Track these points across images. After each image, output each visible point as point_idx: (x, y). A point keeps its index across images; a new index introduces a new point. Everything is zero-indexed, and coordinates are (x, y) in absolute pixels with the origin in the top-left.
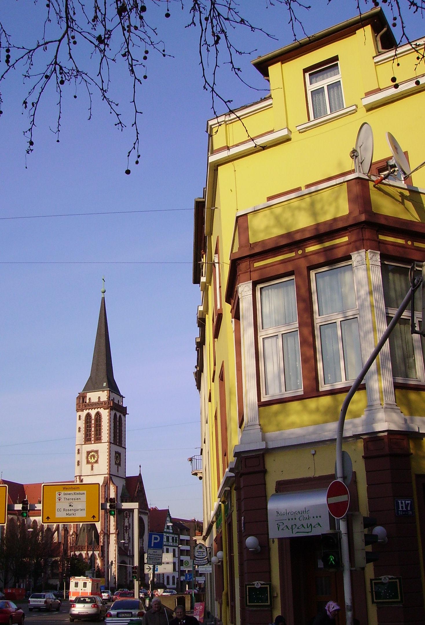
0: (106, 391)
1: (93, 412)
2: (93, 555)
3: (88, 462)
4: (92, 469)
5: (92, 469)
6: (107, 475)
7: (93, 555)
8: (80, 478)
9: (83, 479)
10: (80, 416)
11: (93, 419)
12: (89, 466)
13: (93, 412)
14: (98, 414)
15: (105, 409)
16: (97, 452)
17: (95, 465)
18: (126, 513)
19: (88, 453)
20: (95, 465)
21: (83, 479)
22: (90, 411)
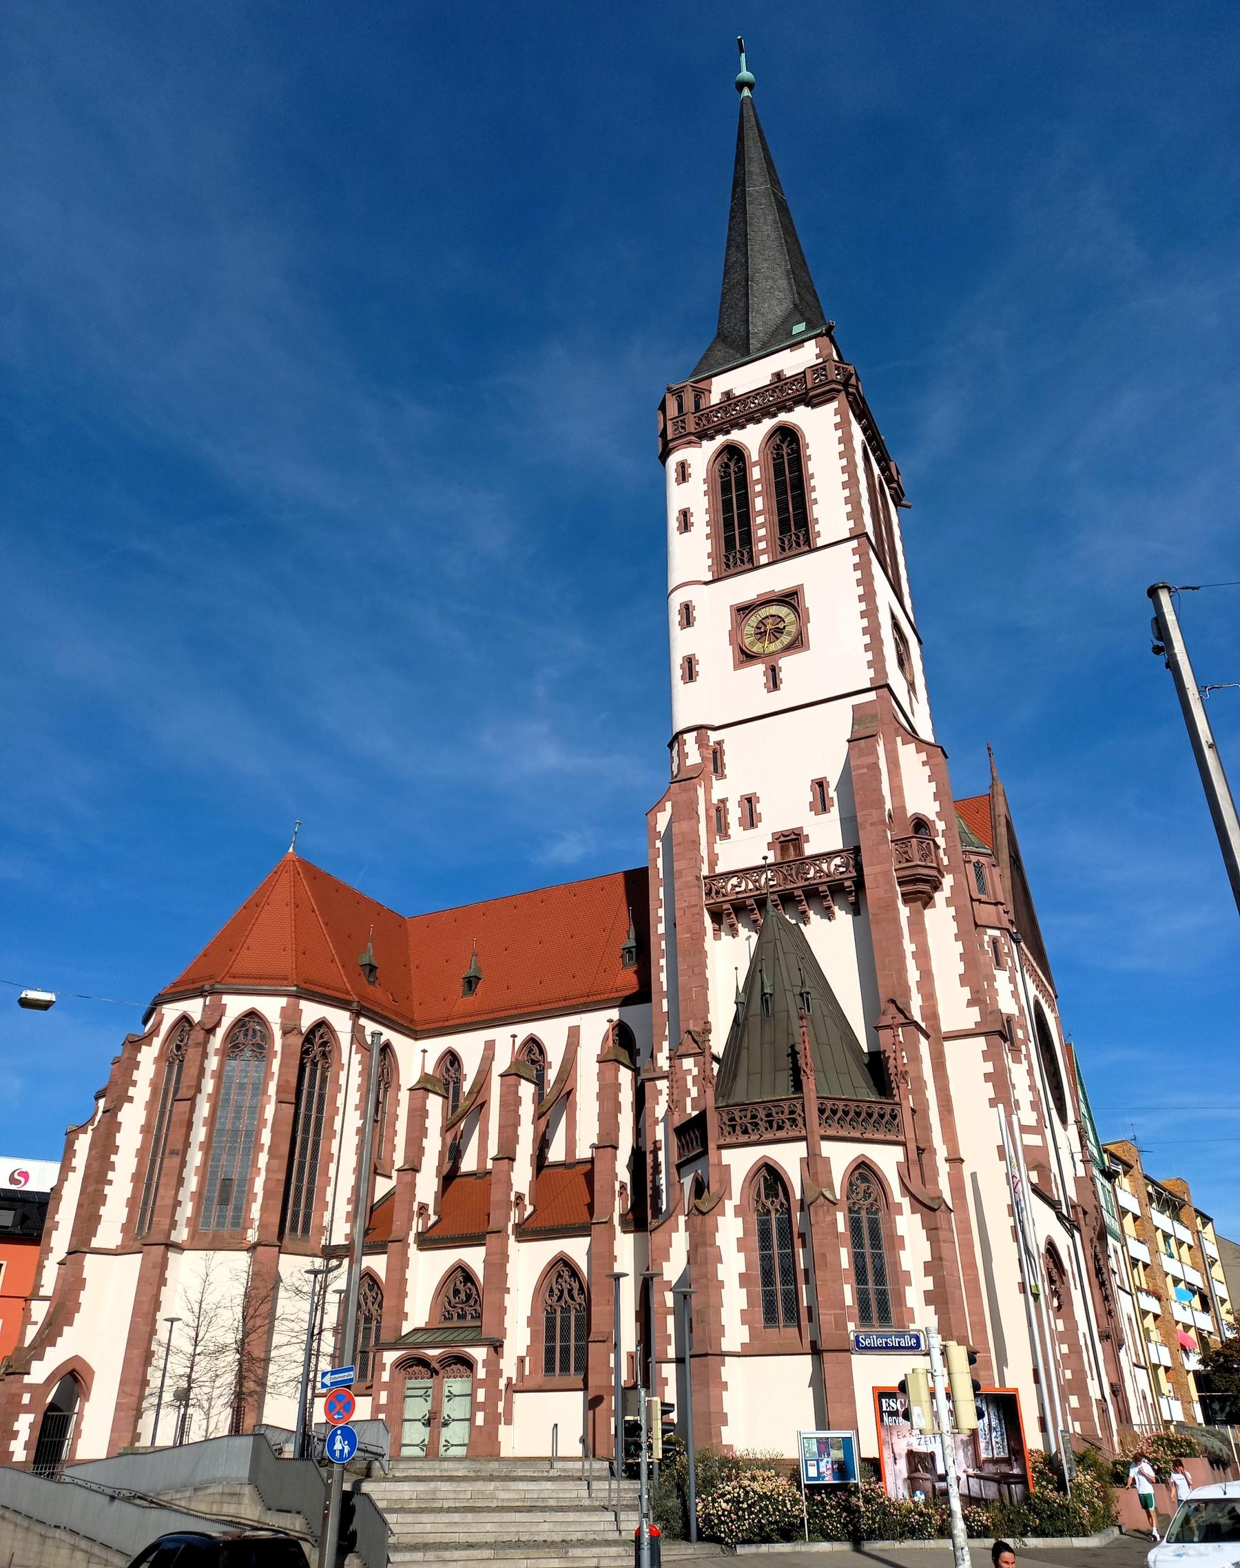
0: (813, 341)
1: (752, 438)
2: (864, 1170)
3: (745, 657)
4: (774, 682)
5: (774, 682)
6: (872, 696)
7: (864, 1170)
8: (702, 743)
9: (720, 743)
10: (683, 466)
11: (755, 464)
12: (757, 671)
13: (752, 438)
14: (788, 437)
15: (814, 406)
16: (791, 598)
17: (787, 664)
18: (995, 942)
19: (743, 610)
20: (787, 664)
21: (720, 743)
22: (736, 435)
